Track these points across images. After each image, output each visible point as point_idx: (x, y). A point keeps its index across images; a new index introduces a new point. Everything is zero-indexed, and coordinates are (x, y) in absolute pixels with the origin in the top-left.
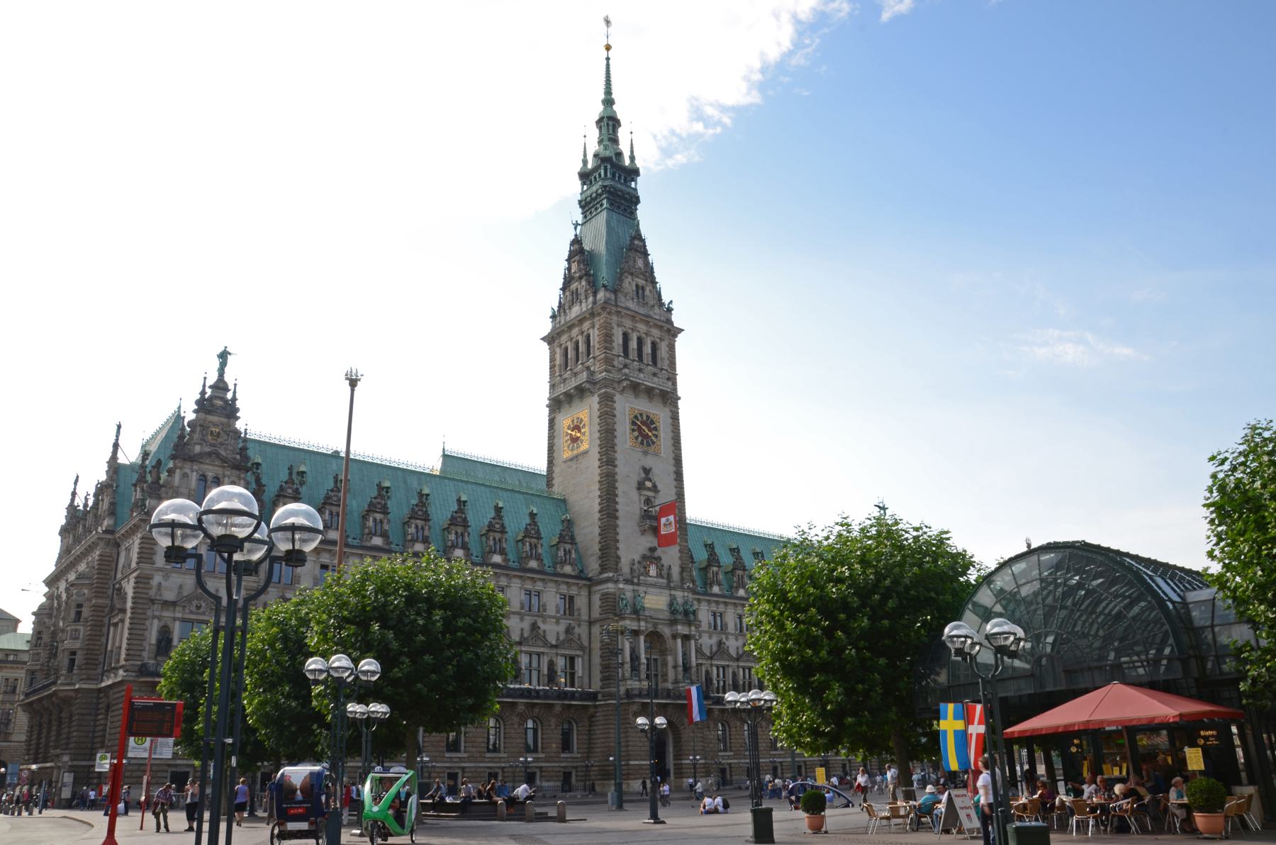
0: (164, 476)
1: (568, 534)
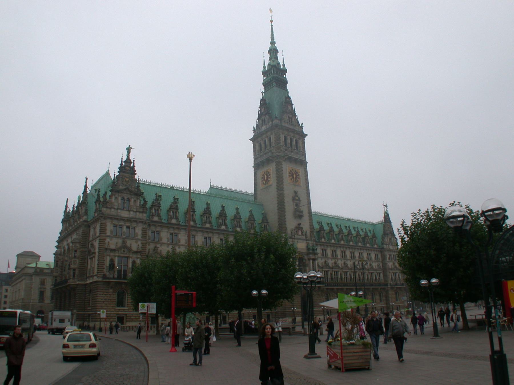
0: (108, 197)
1: (265, 219)
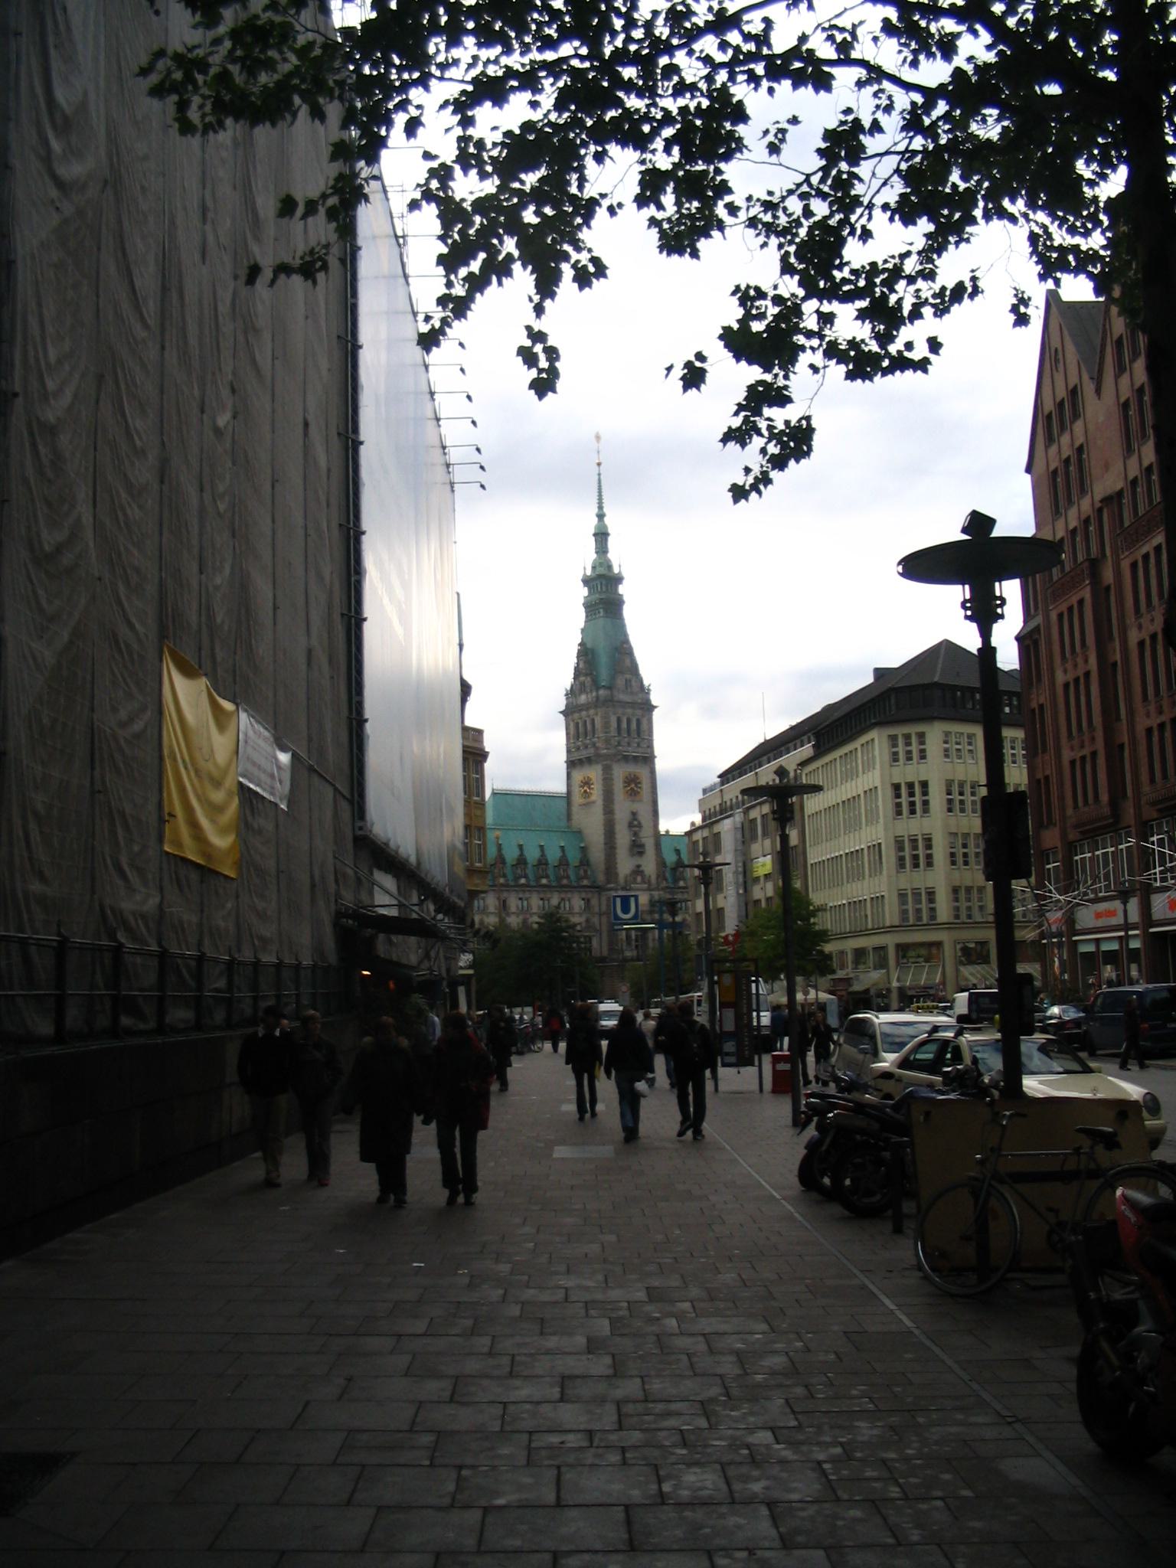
1: (585, 862)
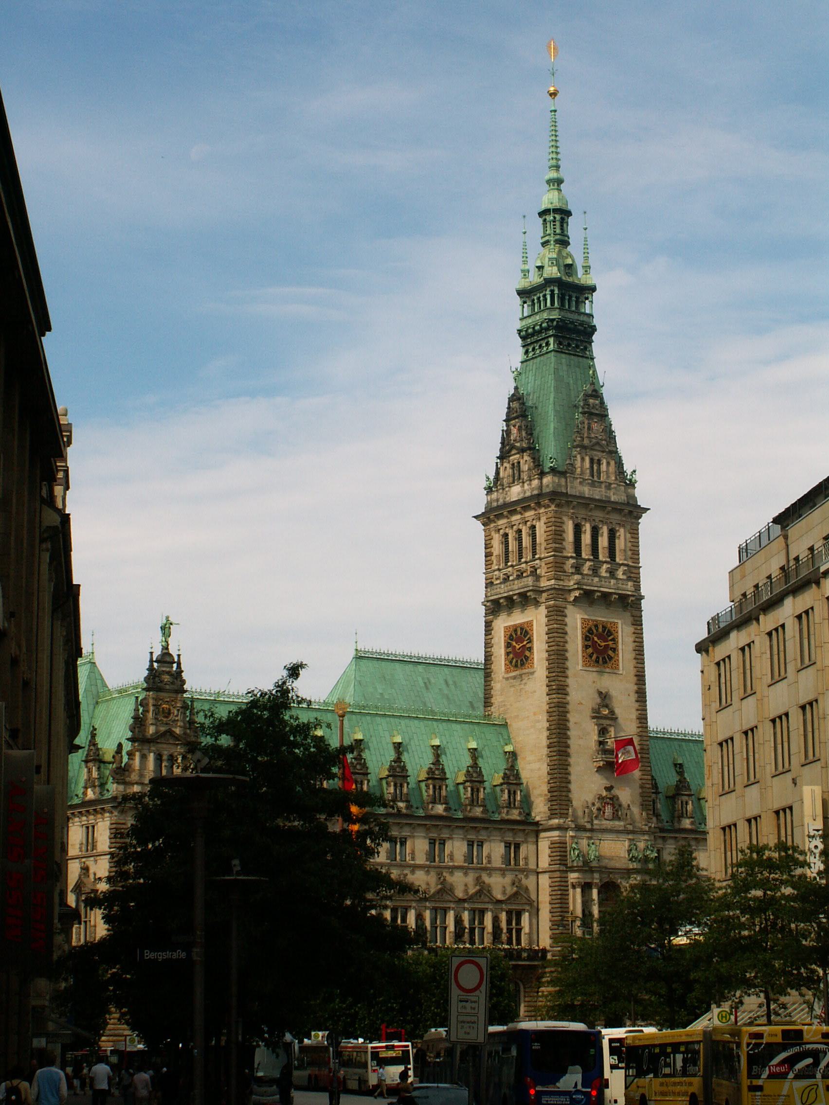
0: (125, 759)
1: (512, 778)
